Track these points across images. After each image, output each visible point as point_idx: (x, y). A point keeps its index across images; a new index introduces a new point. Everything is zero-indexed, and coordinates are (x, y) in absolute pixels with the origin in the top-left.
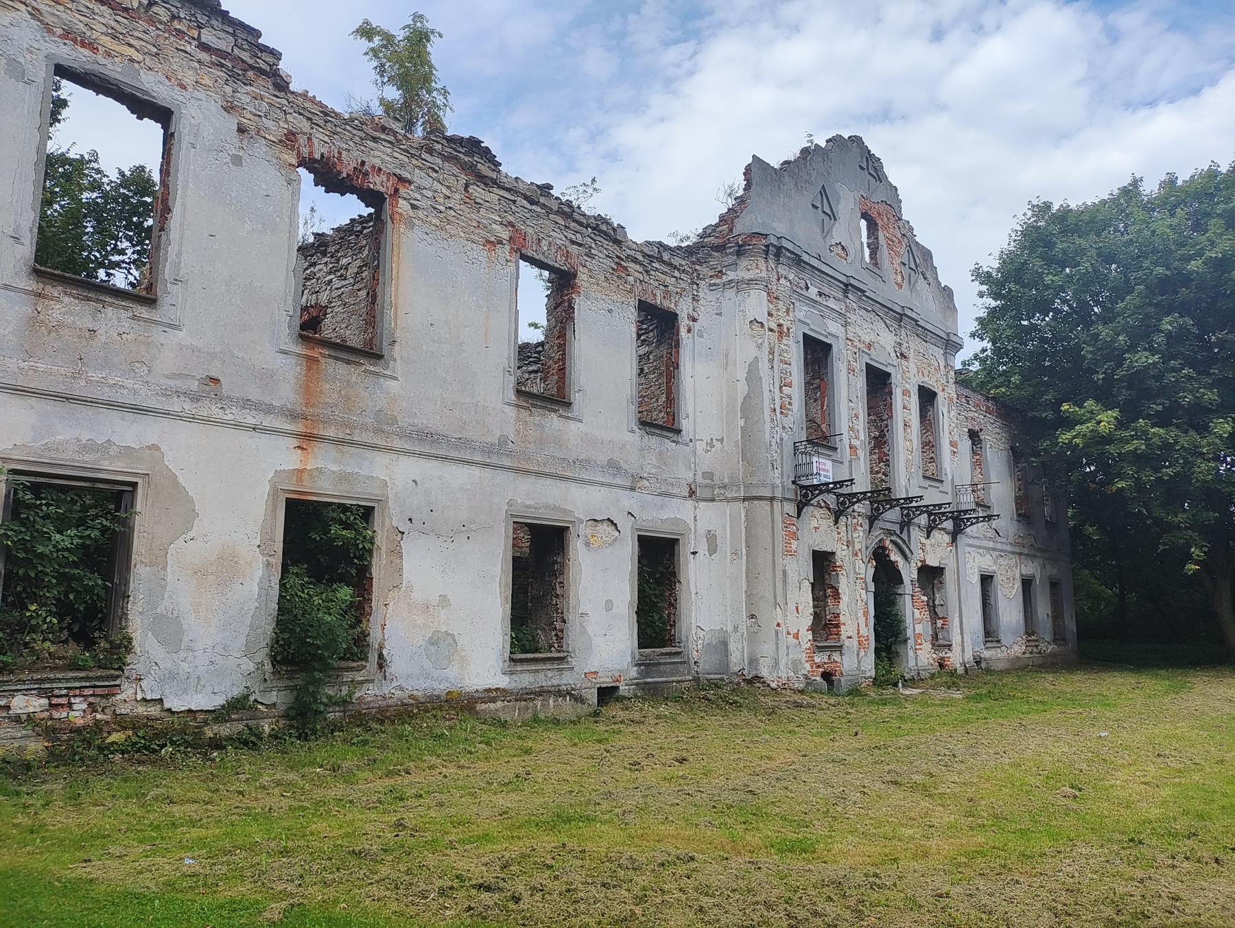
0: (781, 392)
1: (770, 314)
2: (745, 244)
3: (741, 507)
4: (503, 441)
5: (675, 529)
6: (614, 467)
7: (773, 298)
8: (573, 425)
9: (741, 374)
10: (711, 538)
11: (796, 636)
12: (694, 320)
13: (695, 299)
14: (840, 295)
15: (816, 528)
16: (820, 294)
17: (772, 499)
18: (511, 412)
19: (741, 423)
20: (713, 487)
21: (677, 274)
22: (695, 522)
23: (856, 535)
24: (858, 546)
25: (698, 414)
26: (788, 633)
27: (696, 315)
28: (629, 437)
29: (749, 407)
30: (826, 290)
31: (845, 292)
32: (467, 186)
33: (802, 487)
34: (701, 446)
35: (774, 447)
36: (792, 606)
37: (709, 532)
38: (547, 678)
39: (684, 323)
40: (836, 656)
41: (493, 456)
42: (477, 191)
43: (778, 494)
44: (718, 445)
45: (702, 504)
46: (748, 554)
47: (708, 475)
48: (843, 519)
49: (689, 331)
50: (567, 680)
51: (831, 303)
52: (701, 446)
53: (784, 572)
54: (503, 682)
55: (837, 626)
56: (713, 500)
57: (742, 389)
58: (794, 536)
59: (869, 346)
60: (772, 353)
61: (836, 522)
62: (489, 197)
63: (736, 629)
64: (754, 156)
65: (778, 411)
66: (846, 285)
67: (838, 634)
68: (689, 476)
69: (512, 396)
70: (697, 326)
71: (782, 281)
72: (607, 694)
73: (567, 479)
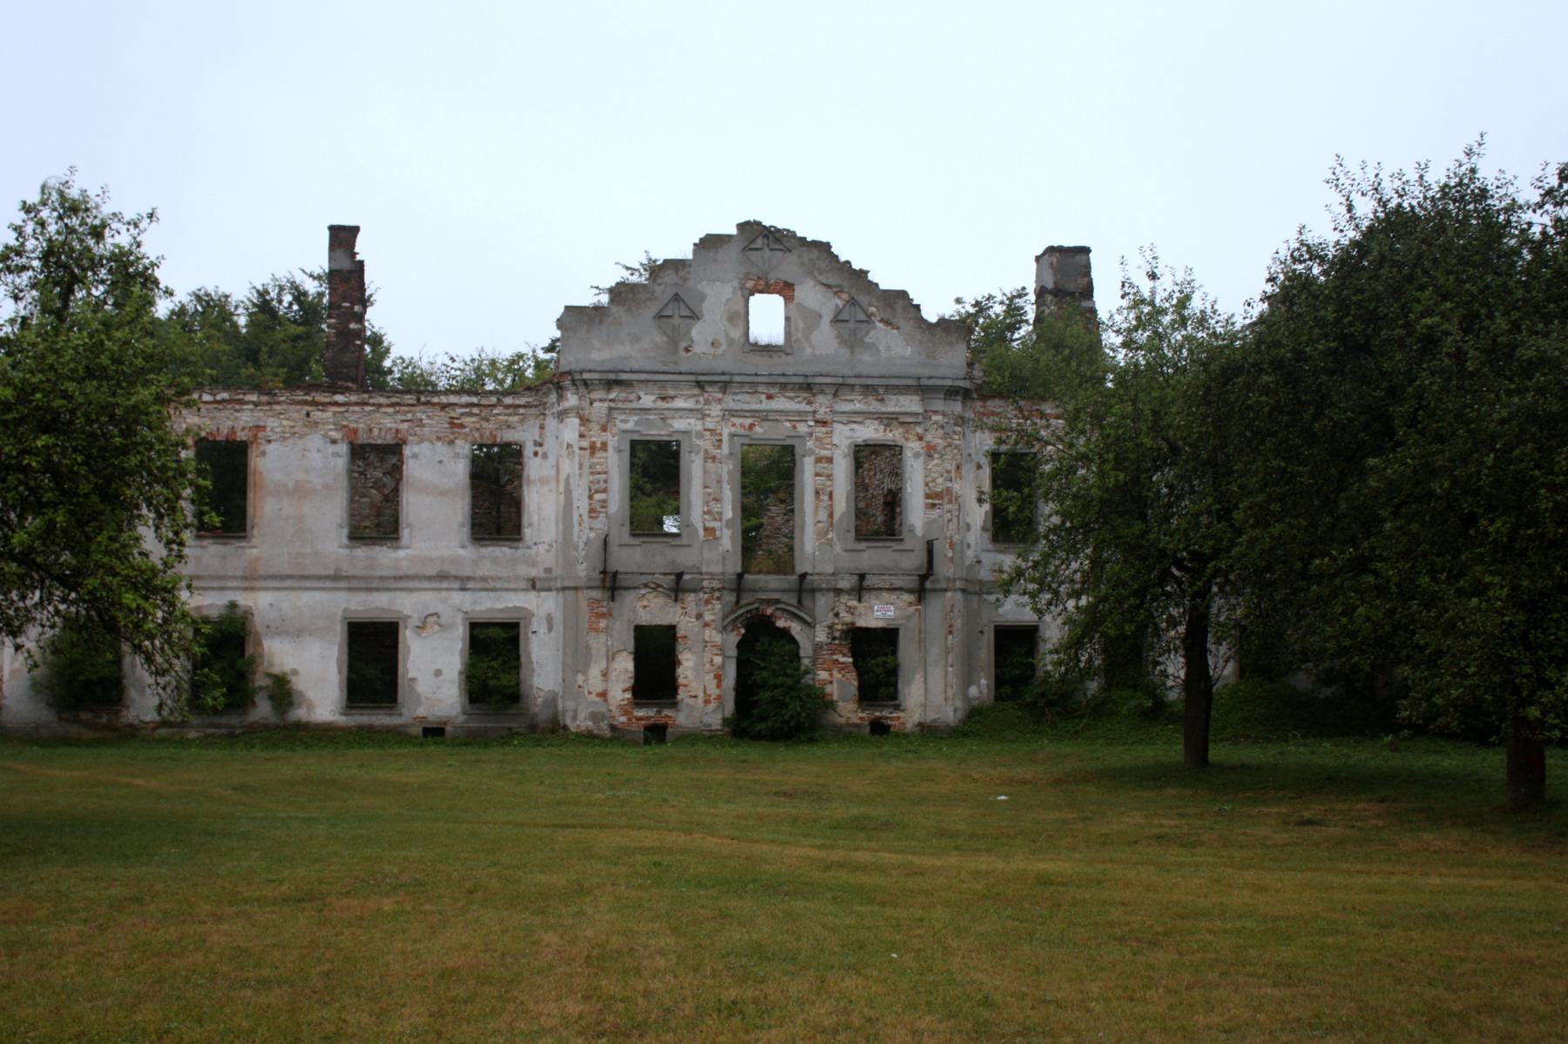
0: (591, 497)
1: (582, 436)
4: (338, 569)
5: (516, 615)
6: (442, 577)
7: (584, 421)
8: (401, 553)
9: (562, 489)
10: (549, 620)
12: (541, 445)
13: (542, 427)
14: (696, 391)
16: (663, 399)
18: (345, 552)
21: (522, 411)
22: (541, 608)
24: (708, 617)
28: (462, 552)
30: (672, 393)
32: (308, 415)
34: (542, 548)
35: (581, 545)
38: (380, 719)
39: (528, 451)
40: (667, 712)
41: (336, 579)
42: (317, 415)
45: (543, 594)
49: (536, 454)
50: (394, 721)
51: (679, 403)
54: (341, 720)
58: (603, 615)
59: (751, 426)
62: (325, 415)
68: (533, 573)
69: (345, 541)
72: (434, 732)
73: (395, 589)
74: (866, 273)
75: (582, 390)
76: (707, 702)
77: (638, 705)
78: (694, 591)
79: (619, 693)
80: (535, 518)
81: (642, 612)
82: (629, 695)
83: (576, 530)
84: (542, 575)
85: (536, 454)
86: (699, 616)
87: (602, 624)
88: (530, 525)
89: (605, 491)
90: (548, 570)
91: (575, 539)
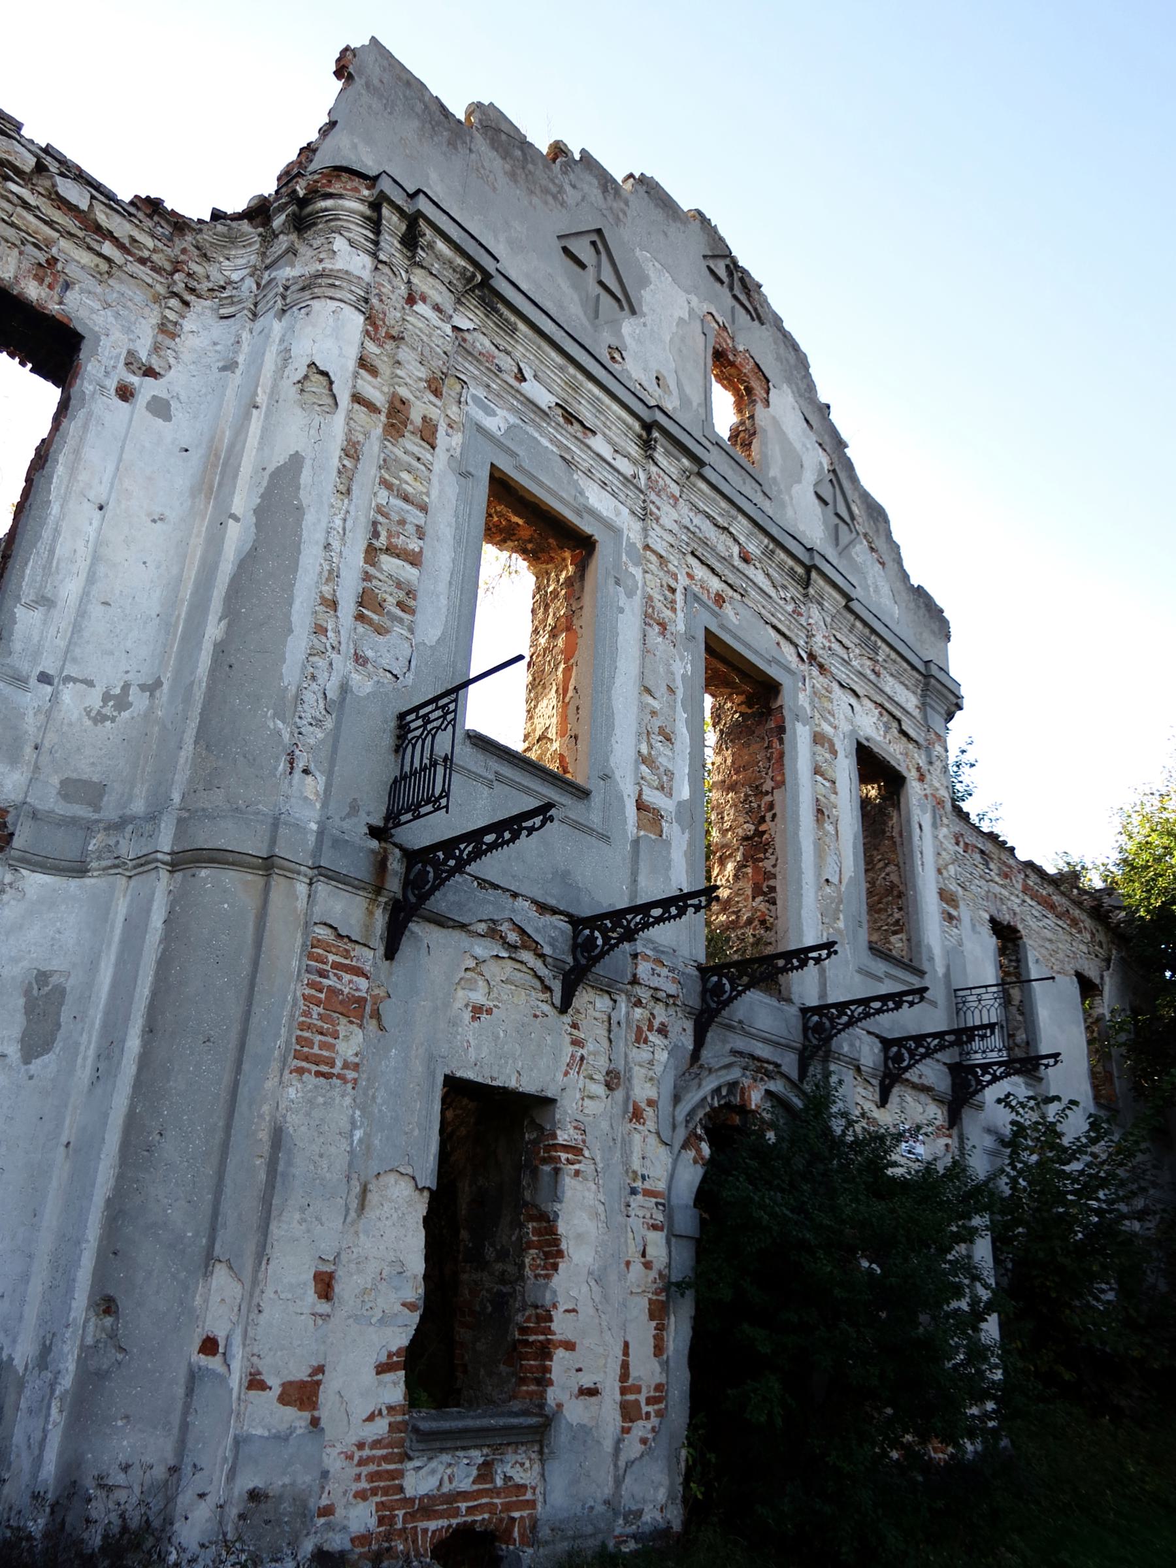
2: (314, 193)
3: (162, 884)
11: (303, 1394)
13: (168, 330)
15: (477, 1011)
17: (268, 865)
19: (214, 630)
20: (89, 828)
21: (108, 248)
23: (643, 1054)
24: (642, 1091)
25: (96, 610)
26: (256, 1383)
27: (156, 364)
29: (253, 588)
31: (647, 445)
33: (411, 856)
36: (291, 1269)
37: (42, 977)
40: (518, 1468)
43: (297, 849)
44: (139, 701)
46: (144, 1060)
47: (72, 789)
48: (583, 998)
52: (73, 702)
53: (278, 1136)
55: (545, 1351)
56: (79, 870)
57: (236, 538)
59: (720, 599)
60: (352, 451)
61: (564, 1007)
63: (45, 1356)
64: (373, 40)
65: (347, 607)
66: (648, 427)
67: (544, 1382)
70: (148, 389)
71: (420, 307)
74: (846, 446)
75: (391, 245)
76: (629, 1413)
77: (434, 1442)
78: (608, 990)
79: (365, 1393)
80: (70, 589)
81: (469, 1030)
82: (394, 1390)
83: (298, 643)
84: (48, 800)
85: (125, 393)
86: (613, 1080)
87: (350, 1042)
88: (46, 602)
89: (414, 559)
90: (92, 793)
91: (290, 673)
